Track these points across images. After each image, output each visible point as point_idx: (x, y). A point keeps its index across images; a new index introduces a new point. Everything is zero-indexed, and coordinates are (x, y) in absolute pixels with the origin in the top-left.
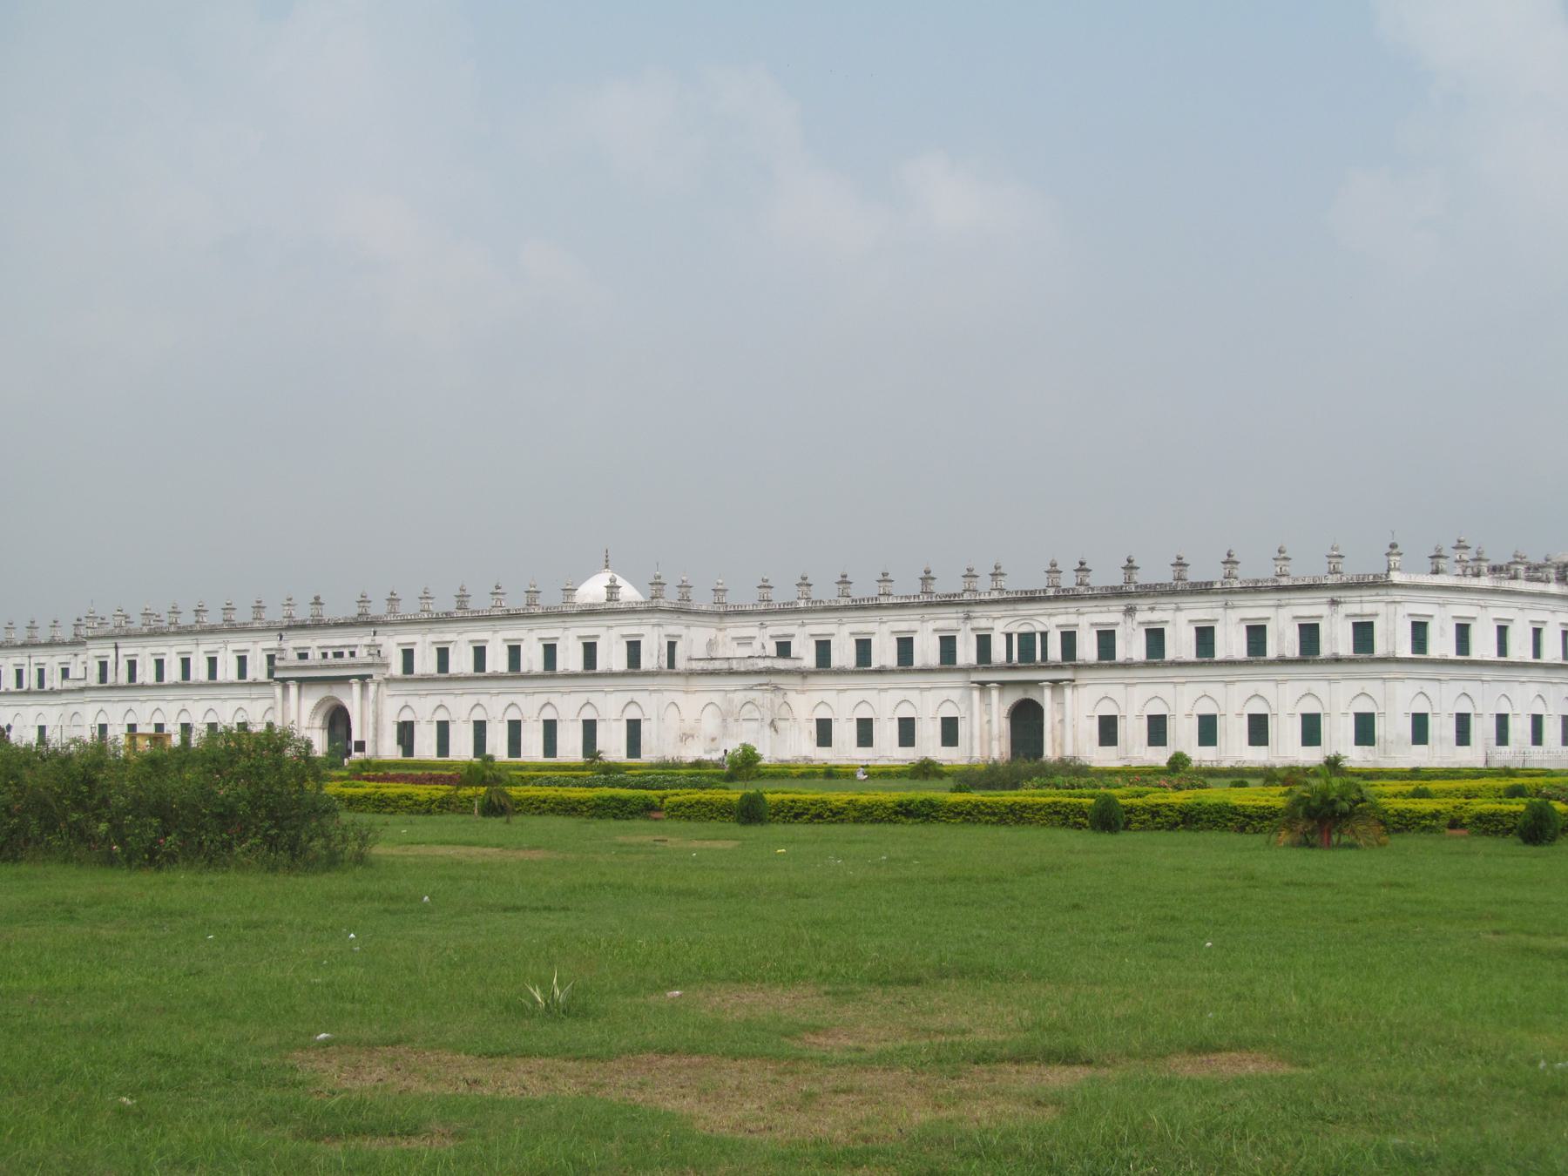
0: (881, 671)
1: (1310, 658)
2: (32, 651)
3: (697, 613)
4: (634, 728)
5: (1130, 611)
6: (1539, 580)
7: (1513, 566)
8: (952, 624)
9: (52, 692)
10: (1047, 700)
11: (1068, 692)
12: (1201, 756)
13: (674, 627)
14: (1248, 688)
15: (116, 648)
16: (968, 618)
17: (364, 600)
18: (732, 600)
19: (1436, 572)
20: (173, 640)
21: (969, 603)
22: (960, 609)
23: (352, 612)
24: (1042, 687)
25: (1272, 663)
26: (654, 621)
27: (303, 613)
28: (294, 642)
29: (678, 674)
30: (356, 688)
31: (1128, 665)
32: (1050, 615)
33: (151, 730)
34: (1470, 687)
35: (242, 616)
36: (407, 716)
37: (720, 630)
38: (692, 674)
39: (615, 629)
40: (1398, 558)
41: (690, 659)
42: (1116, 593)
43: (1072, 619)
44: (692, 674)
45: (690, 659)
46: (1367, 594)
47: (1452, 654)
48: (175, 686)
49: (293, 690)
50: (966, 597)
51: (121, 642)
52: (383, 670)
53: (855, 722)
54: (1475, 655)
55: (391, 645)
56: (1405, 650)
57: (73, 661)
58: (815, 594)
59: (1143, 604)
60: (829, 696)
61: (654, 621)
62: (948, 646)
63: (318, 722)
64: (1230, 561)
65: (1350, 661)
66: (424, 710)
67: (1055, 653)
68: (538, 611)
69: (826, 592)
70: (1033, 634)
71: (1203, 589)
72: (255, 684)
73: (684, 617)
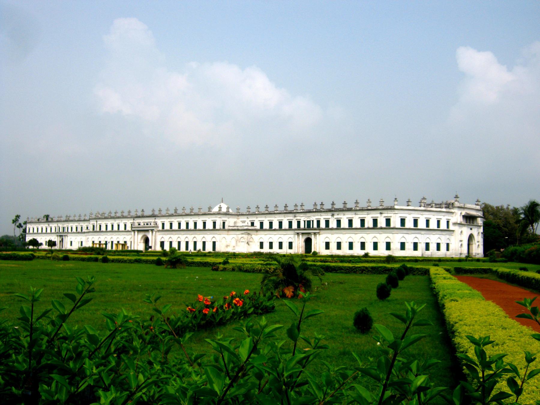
0: (275, 230)
1: (375, 227)
2: (80, 222)
3: (231, 215)
4: (214, 243)
5: (333, 215)
6: (440, 208)
7: (432, 204)
8: (291, 218)
9: (84, 233)
10: (313, 237)
11: (318, 235)
12: (372, 253)
13: (225, 218)
14: (360, 235)
15: (97, 222)
16: (295, 217)
17: (153, 211)
18: (241, 211)
19: (408, 206)
20: (110, 220)
21: (295, 213)
22: (293, 214)
23: (150, 213)
24: (312, 234)
25: (366, 229)
26: (219, 217)
27: (139, 214)
28: (137, 221)
29: (225, 230)
30: (151, 233)
31: (332, 229)
32: (314, 216)
33: (123, 243)
34: (417, 236)
35: (126, 214)
36: (163, 240)
37: (238, 219)
38: (229, 230)
40: (396, 202)
41: (229, 226)
42: (330, 211)
43: (319, 217)
44: (229, 230)
45: (229, 226)
46: (389, 211)
47: (412, 227)
48: (110, 231)
49: (136, 233)
50: (295, 211)
51: (98, 220)
52: (157, 228)
53: (269, 243)
54: (419, 227)
55: (159, 221)
56: (398, 225)
57: (89, 225)
58: (260, 210)
59: (336, 213)
60: (263, 236)
61: (219, 217)
62: (290, 223)
63: (142, 241)
64: (357, 203)
65: (385, 228)
66: (166, 238)
67: (315, 226)
68: (193, 214)
69: (263, 210)
70: (310, 221)
71: (350, 210)
72: (128, 231)
73: (227, 216)
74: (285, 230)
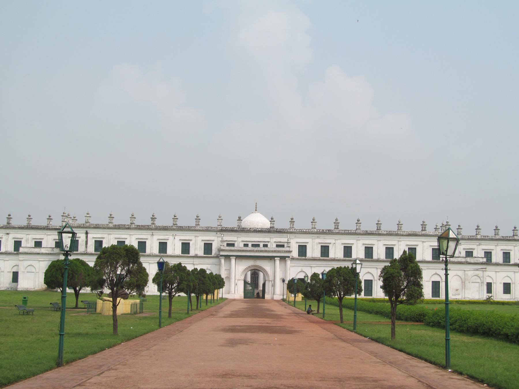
39: (427, 243)
49: (233, 261)
53: (502, 284)
74: (497, 264)
